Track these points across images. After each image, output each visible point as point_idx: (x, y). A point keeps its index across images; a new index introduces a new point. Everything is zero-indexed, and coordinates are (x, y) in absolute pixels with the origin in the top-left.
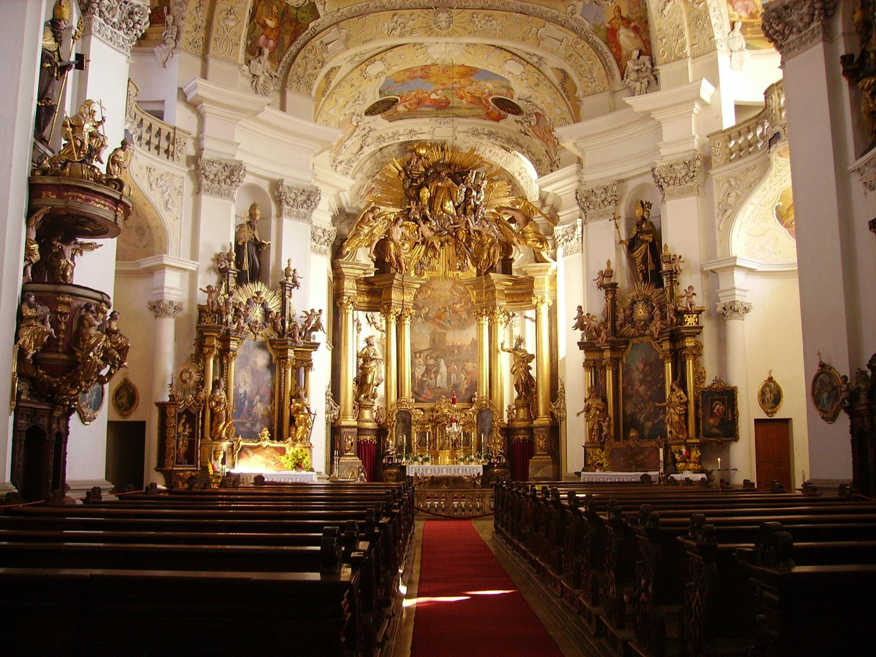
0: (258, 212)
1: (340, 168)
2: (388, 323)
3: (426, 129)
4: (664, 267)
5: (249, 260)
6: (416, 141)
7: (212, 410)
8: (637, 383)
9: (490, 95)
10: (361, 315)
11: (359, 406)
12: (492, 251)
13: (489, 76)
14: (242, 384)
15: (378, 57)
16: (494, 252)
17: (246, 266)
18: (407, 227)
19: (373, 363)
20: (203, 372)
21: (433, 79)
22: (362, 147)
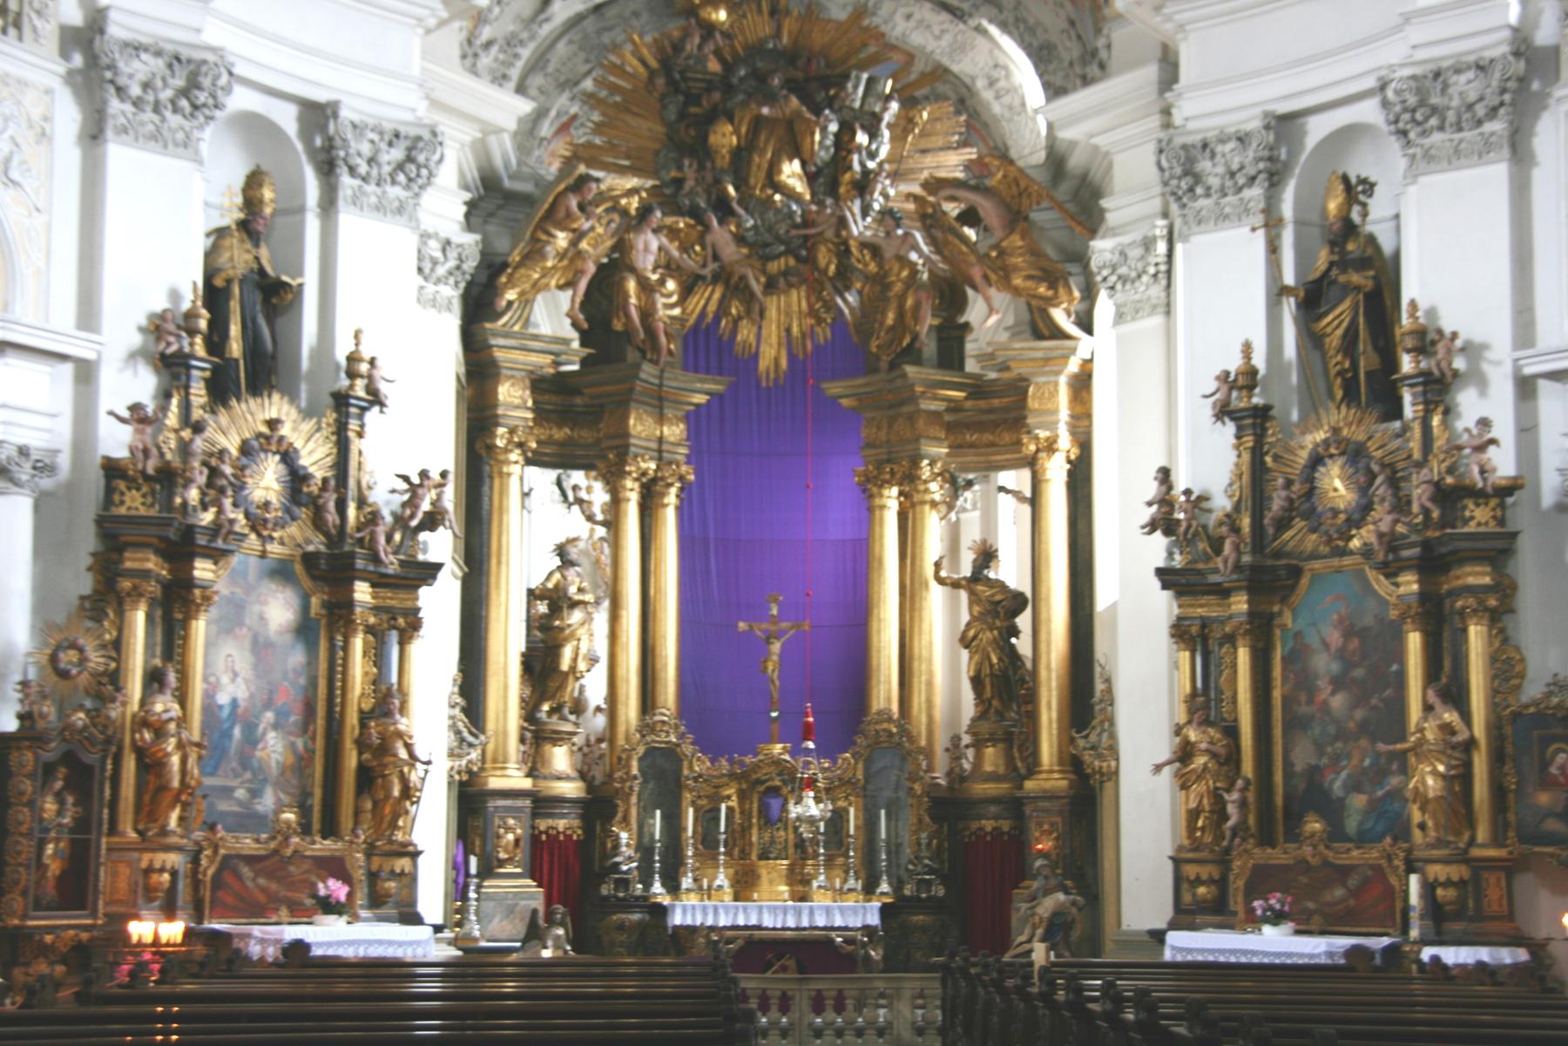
0: (268, 194)
1: (486, 61)
2: (616, 502)
4: (1407, 364)
5: (242, 327)
7: (140, 752)
8: (1323, 684)
10: (542, 479)
11: (537, 737)
12: (909, 302)
14: (225, 679)
16: (917, 306)
17: (235, 348)
18: (673, 233)
19: (576, 616)
20: (117, 647)
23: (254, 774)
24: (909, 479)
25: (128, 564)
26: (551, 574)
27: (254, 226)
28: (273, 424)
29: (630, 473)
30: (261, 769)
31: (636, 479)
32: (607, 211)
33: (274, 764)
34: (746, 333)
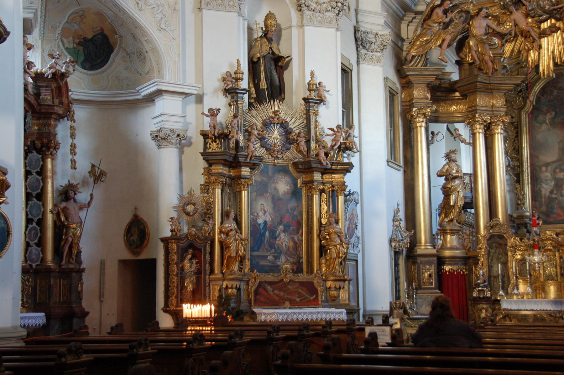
2: (473, 135)
14: (261, 214)
18: (496, 18)
19: (457, 182)
23: (276, 250)
25: (213, 171)
26: (444, 166)
27: (269, 36)
28: (275, 112)
29: (478, 121)
30: (278, 247)
31: (482, 124)
32: (459, 12)
33: (284, 246)
34: (532, 55)
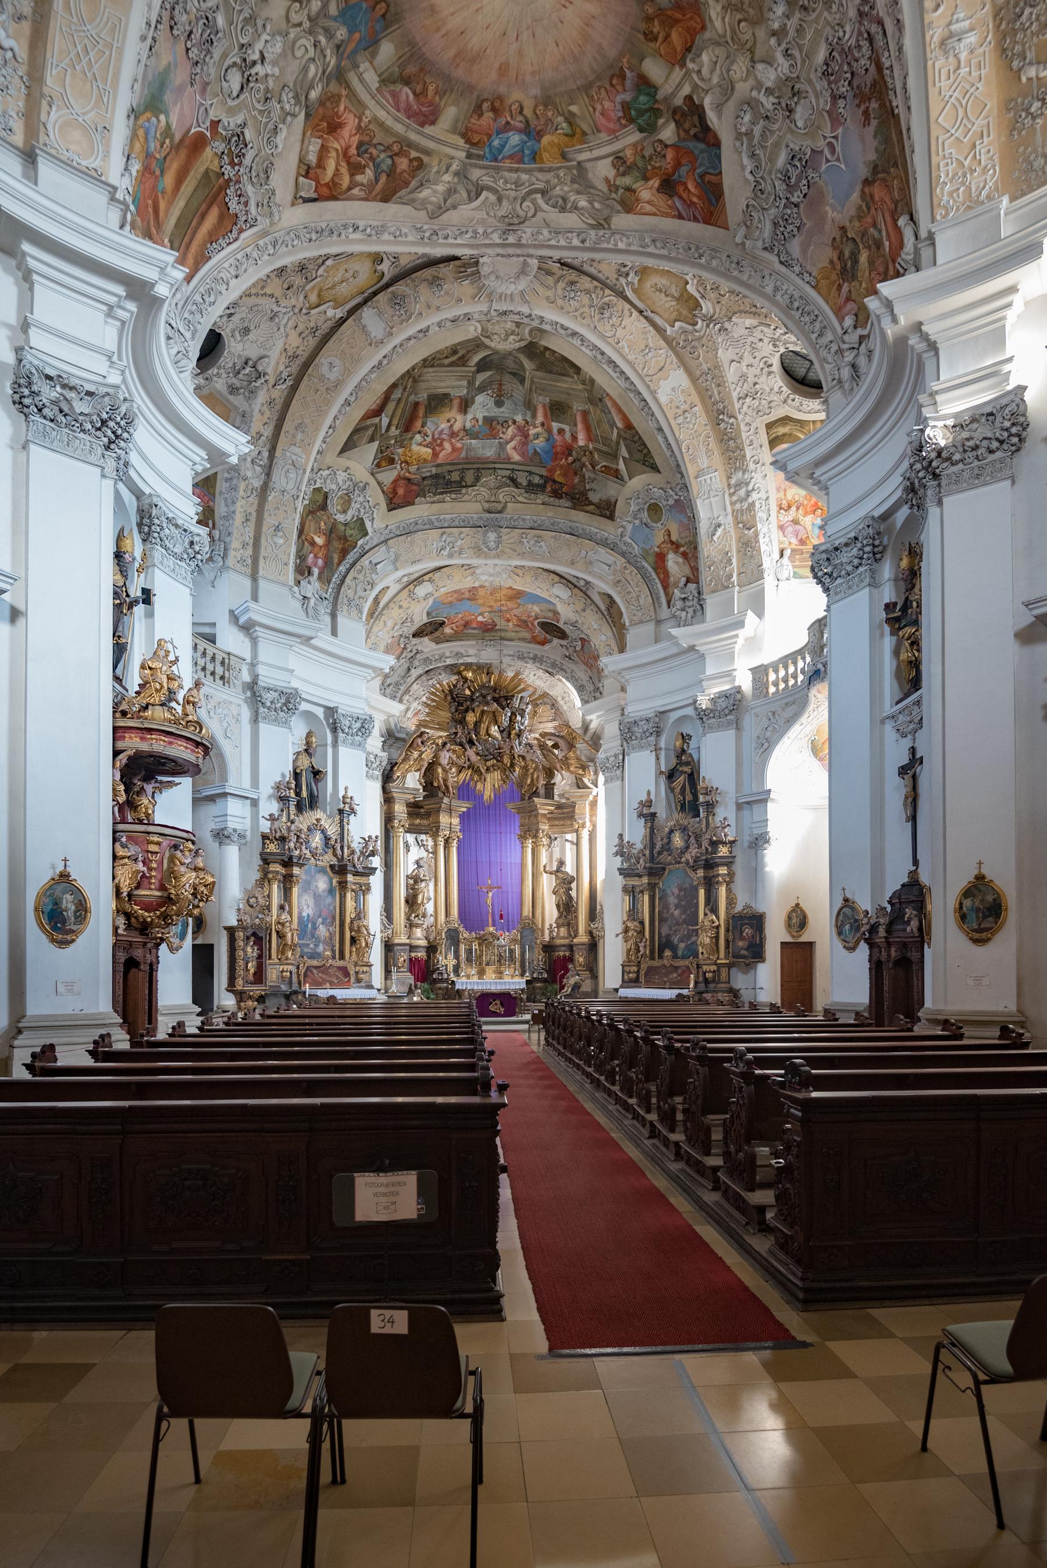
3: (471, 652)
6: (462, 664)
9: (537, 618)
13: (536, 599)
15: (426, 578)
18: (454, 751)
21: (480, 601)
22: (409, 669)
24: (536, 836)
34: (479, 786)
